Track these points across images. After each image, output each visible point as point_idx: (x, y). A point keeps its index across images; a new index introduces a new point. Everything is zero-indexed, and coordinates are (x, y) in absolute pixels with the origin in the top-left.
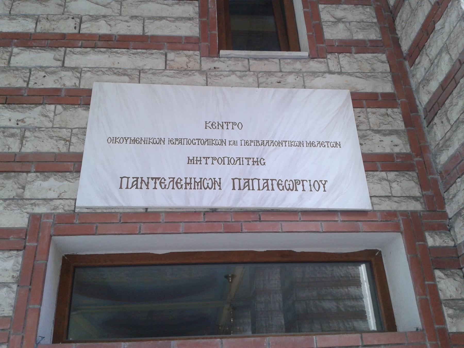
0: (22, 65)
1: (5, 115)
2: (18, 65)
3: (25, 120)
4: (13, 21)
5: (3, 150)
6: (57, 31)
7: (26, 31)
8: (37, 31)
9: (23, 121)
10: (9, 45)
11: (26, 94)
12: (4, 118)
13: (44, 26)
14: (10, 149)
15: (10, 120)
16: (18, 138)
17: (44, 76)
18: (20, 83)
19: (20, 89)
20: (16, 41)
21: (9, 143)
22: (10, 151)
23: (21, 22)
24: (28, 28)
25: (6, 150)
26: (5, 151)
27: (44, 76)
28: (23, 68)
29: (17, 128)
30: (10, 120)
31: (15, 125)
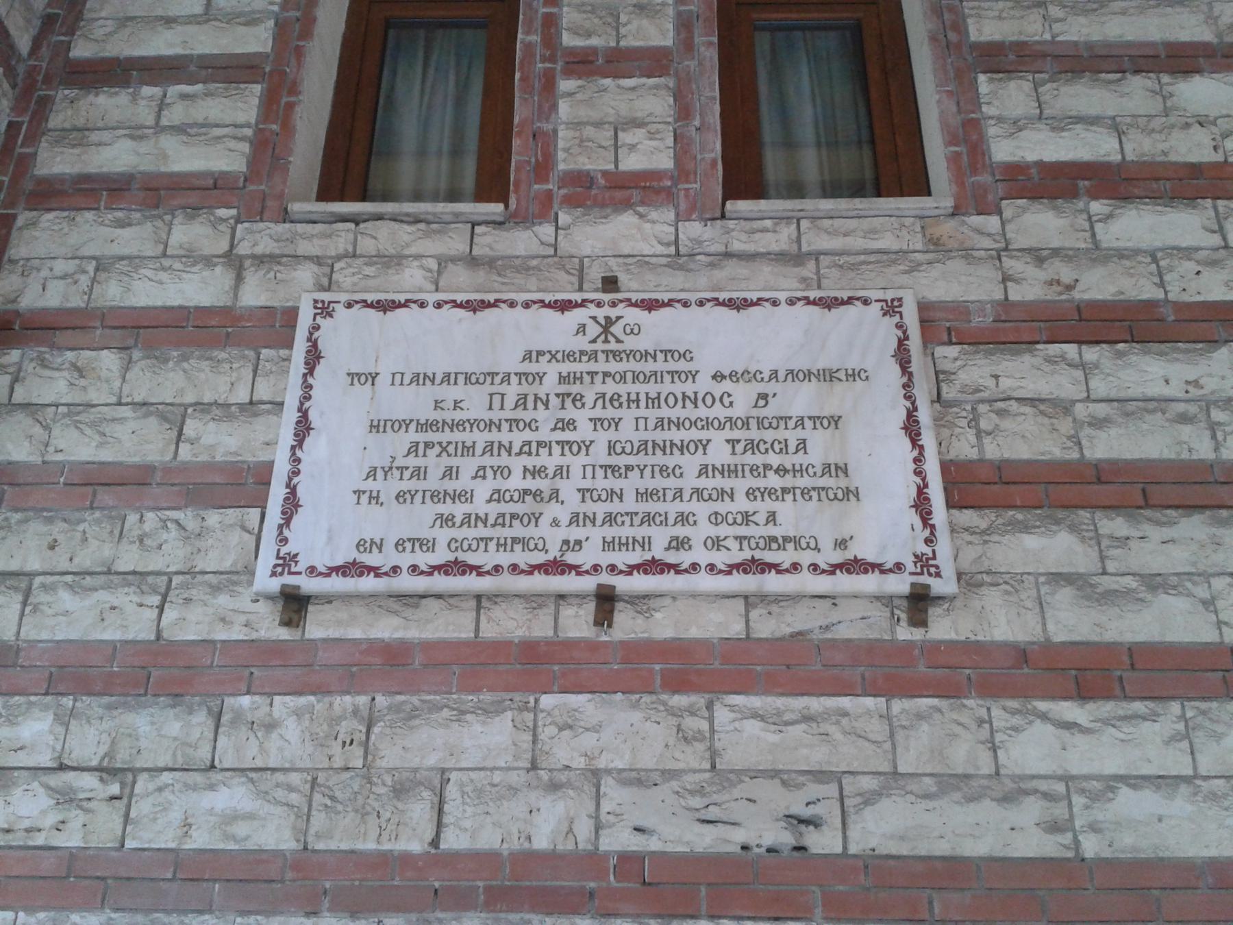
0: (1129, 244)
1: (1149, 369)
2: (1121, 244)
3: (1202, 382)
4: (1063, 134)
5: (1178, 454)
6: (1173, 158)
7: (1102, 159)
8: (1128, 158)
9: (1196, 383)
10: (1073, 194)
11: (1172, 318)
12: (1150, 377)
13: (1139, 147)
14: (1194, 452)
15: (1167, 382)
16: (1202, 424)
17: (1198, 273)
18: (1148, 291)
19: (1150, 305)
20: (1086, 183)
21: (1186, 439)
22: (1195, 457)
23: (1082, 136)
24: (1102, 152)
25: (1185, 455)
26: (1183, 456)
27: (1198, 273)
28: (1137, 252)
29: (1187, 401)
30: (1167, 382)
31: (1181, 395)
